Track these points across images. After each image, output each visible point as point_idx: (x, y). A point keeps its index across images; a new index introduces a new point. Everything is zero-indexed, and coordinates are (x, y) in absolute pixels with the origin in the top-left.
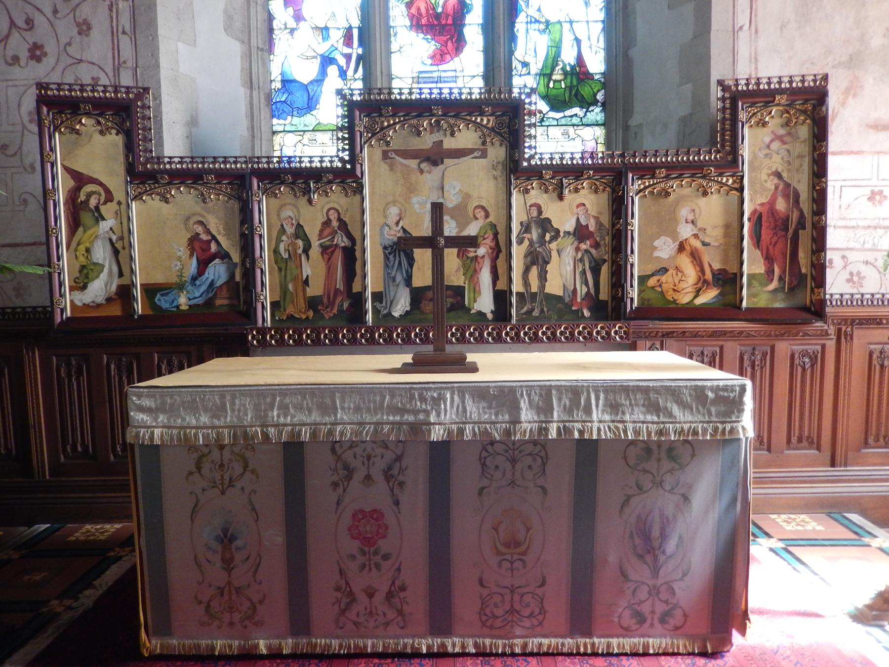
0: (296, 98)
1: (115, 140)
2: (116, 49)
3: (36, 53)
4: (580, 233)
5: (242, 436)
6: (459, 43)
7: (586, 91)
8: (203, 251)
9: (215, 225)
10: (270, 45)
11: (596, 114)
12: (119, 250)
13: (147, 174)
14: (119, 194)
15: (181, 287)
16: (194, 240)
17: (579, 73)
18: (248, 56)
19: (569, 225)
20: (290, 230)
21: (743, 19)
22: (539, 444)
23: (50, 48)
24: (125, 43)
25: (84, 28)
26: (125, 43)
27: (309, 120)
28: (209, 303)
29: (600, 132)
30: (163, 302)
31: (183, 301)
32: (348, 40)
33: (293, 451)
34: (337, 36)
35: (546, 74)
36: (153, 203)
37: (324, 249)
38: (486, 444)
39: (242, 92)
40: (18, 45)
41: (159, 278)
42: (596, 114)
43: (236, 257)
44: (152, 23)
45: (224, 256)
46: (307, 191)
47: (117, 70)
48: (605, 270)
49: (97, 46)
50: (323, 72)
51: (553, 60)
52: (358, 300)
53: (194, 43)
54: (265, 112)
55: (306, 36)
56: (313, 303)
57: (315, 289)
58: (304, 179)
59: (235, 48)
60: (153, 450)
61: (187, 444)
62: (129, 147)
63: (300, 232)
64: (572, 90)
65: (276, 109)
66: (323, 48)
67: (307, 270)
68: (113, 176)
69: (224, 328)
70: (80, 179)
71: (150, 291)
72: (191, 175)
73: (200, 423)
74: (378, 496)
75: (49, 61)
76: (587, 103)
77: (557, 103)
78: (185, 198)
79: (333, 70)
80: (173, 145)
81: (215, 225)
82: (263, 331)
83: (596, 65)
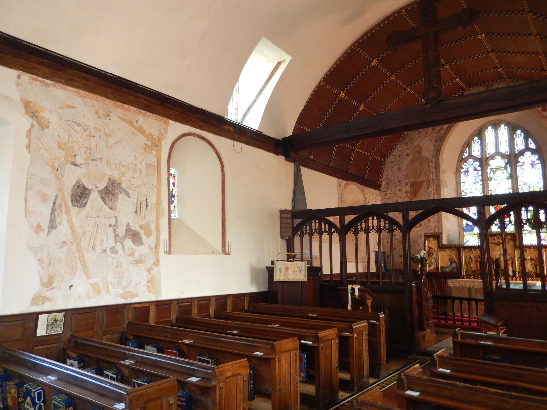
1: (436, 241)
2: (435, 224)
4: (532, 259)
5: (463, 287)
8: (451, 261)
9: (454, 256)
12: (437, 260)
13: (441, 247)
14: (436, 251)
15: (447, 267)
16: (450, 259)
19: (529, 258)
20: (468, 257)
26: (436, 223)
27: (472, 232)
28: (453, 270)
30: (444, 270)
31: (448, 270)
36: (442, 252)
37: (476, 261)
39: (457, 228)
41: (443, 266)
43: (458, 262)
44: (441, 220)
45: (455, 262)
46: (472, 250)
47: (435, 228)
48: (538, 267)
53: (448, 221)
54: (462, 231)
56: (473, 271)
57: (474, 269)
58: (471, 248)
60: (451, 287)
61: (455, 287)
62: (439, 243)
63: (470, 258)
67: (472, 265)
68: (436, 248)
69: (456, 274)
70: (430, 248)
71: (442, 268)
72: (449, 247)
75: (422, 227)
78: (448, 251)
80: (445, 242)
81: (454, 256)
82: (463, 276)
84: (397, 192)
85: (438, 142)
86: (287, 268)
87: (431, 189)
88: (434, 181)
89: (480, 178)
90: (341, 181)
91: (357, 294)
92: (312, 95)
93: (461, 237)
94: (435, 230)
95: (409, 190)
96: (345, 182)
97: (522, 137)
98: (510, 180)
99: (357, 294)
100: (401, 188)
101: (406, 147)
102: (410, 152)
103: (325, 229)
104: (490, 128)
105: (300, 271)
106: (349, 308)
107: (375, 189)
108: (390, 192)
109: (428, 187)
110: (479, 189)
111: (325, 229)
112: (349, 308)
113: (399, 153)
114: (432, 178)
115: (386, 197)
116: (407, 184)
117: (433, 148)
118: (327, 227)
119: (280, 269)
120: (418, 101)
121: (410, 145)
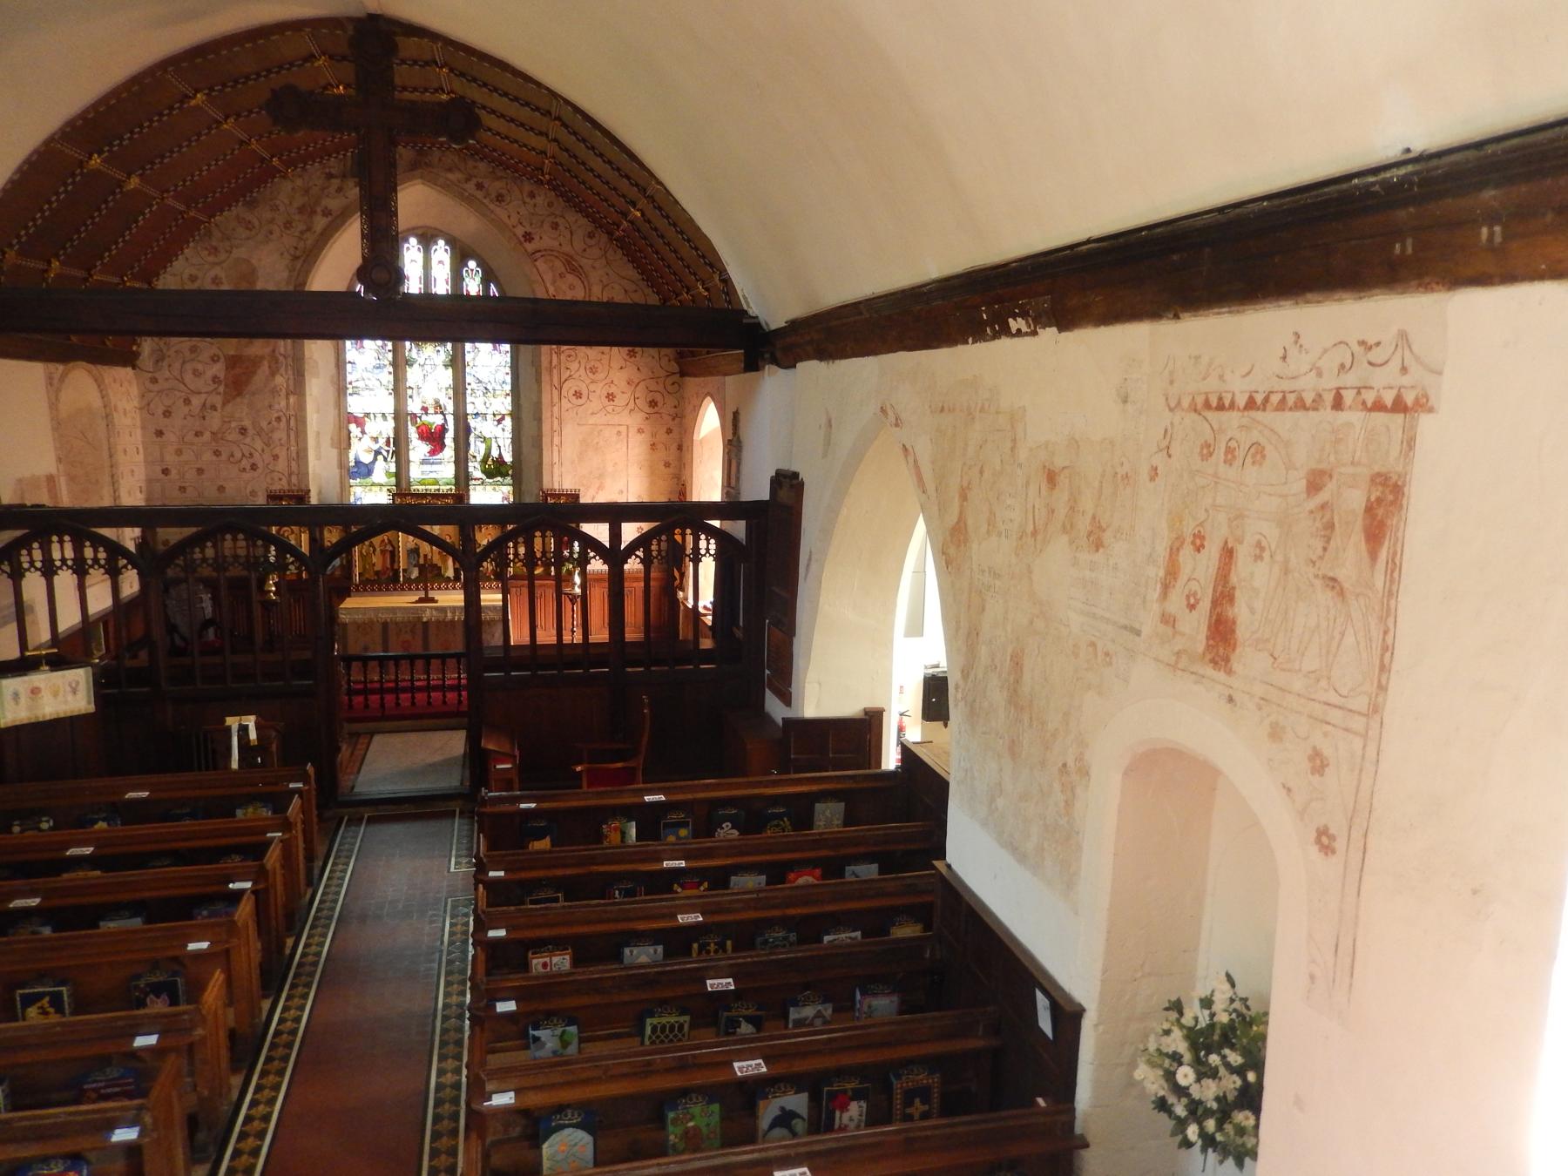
0: (364, 470)
3: (254, 467)
6: (442, 446)
7: (503, 470)
10: (349, 445)
11: (509, 480)
17: (500, 461)
18: (340, 454)
21: (556, 459)
22: (452, 621)
23: (260, 465)
24: (294, 464)
25: (276, 457)
26: (294, 464)
27: (368, 480)
29: (510, 488)
32: (388, 443)
33: (385, 625)
34: (382, 442)
35: (484, 461)
38: (438, 622)
40: (245, 463)
42: (509, 480)
49: (281, 465)
50: (375, 459)
51: (487, 455)
52: (396, 572)
55: (367, 442)
56: (377, 573)
57: (378, 567)
59: (335, 452)
61: (355, 623)
64: (495, 469)
65: (353, 475)
66: (376, 447)
73: (359, 617)
74: (408, 637)
76: (504, 475)
77: (490, 474)
79: (380, 458)
83: (508, 458)
84: (188, 377)
85: (298, 264)
86: (35, 691)
87: (279, 380)
88: (290, 361)
89: (390, 356)
90: (52, 366)
91: (253, 735)
92: (19, 170)
93: (344, 489)
94: (289, 483)
95: (222, 376)
96: (61, 367)
97: (478, 279)
98: (450, 370)
99: (253, 735)
100: (200, 367)
101: (211, 259)
102: (222, 275)
103: (96, 560)
104: (413, 241)
105: (74, 692)
106: (235, 765)
107: (125, 365)
108: (167, 374)
109: (273, 374)
110: (385, 382)
111: (96, 560)
112: (235, 765)
113: (194, 272)
114: (282, 350)
115: (155, 388)
116: (215, 359)
117: (286, 274)
118: (102, 555)
119: (16, 696)
120: (263, 160)
121: (223, 256)
